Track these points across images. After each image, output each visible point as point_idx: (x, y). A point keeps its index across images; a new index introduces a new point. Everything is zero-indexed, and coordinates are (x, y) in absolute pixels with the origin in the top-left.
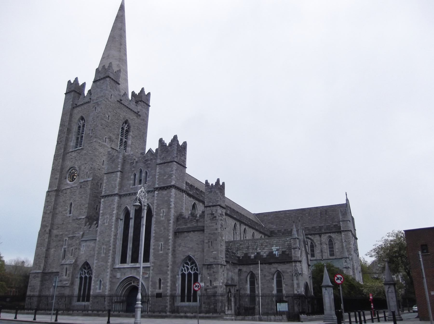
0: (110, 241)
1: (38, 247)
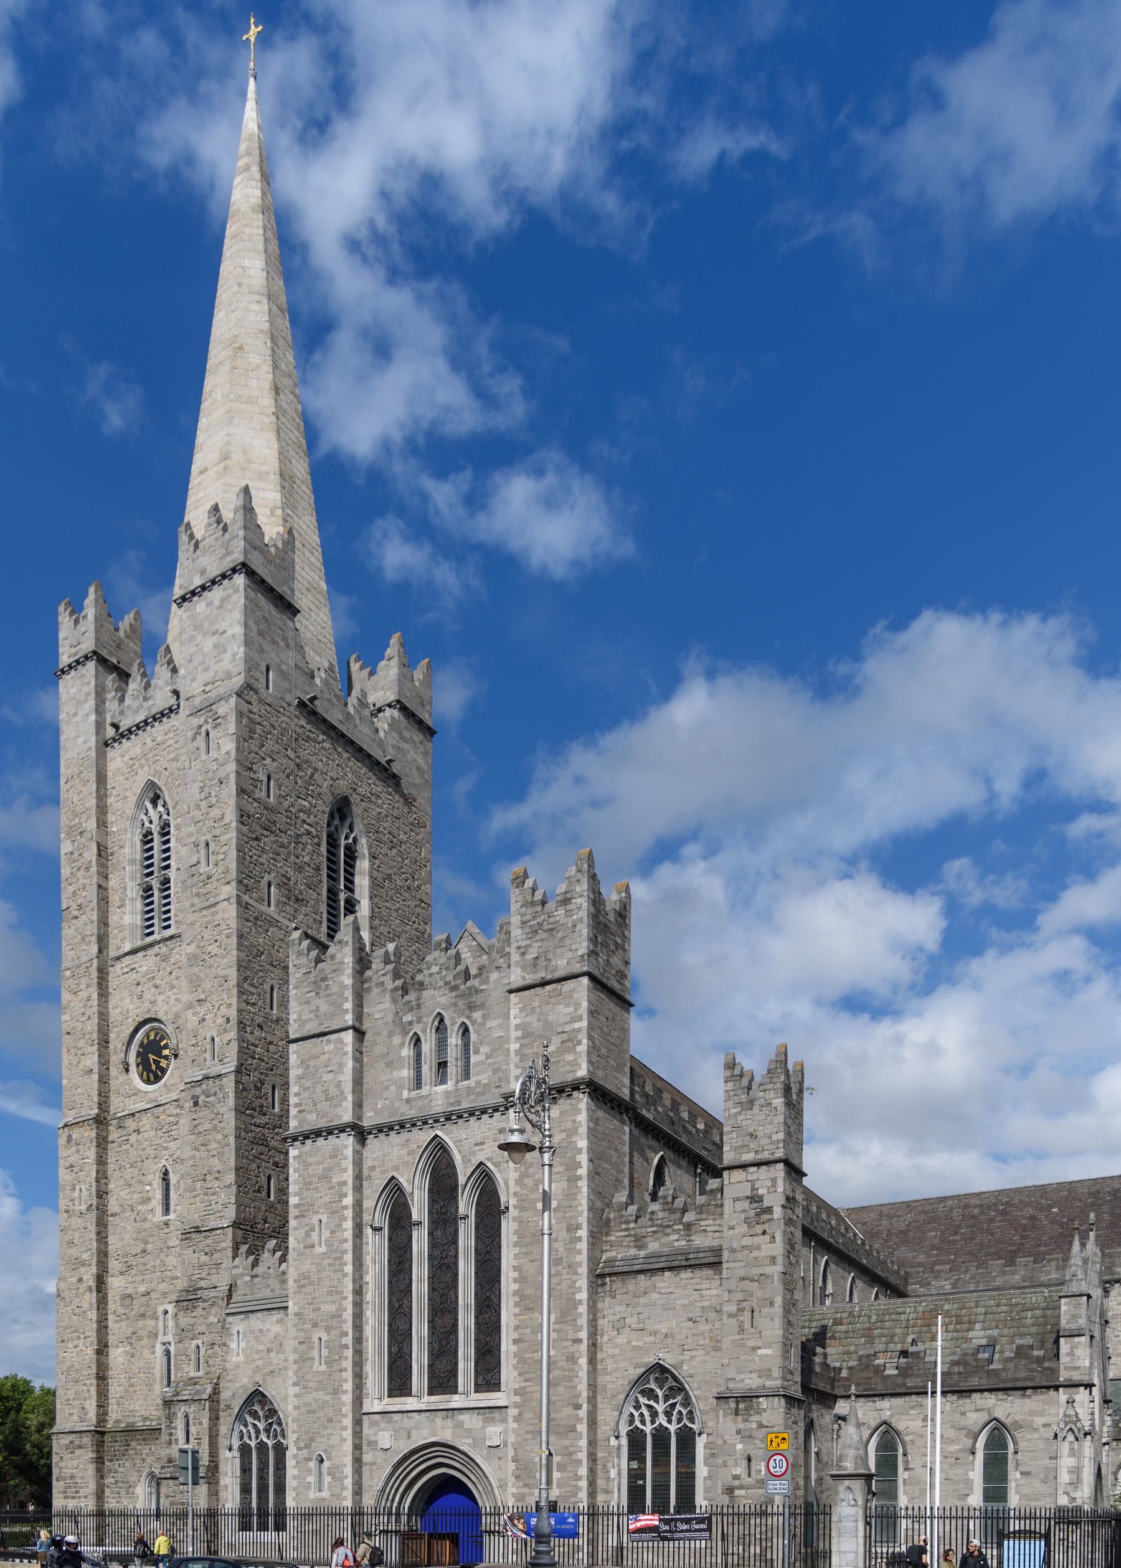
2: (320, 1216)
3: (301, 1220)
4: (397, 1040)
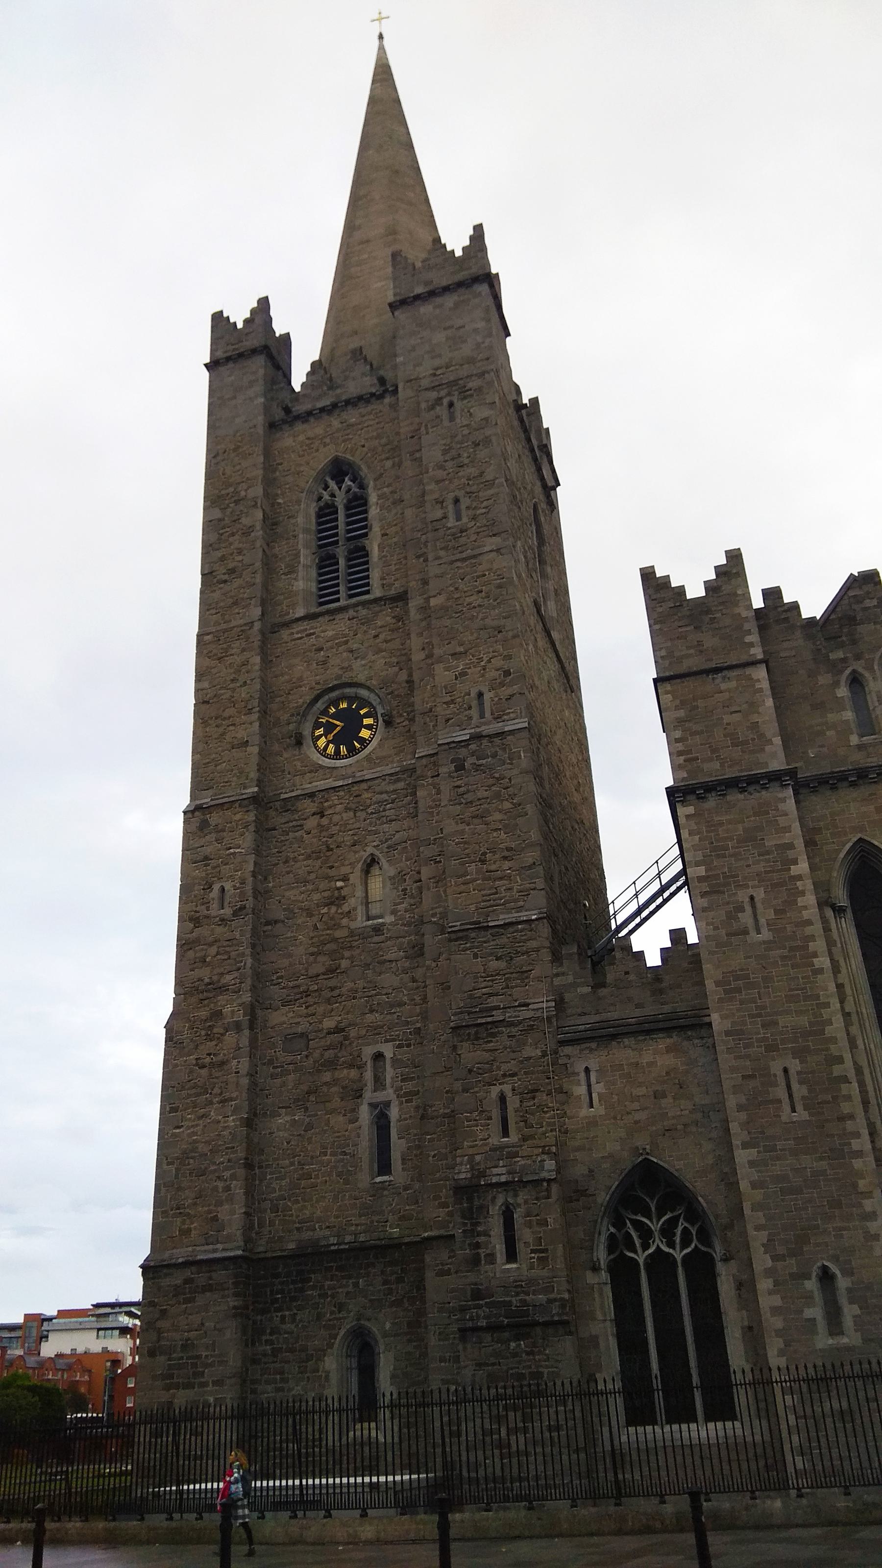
0: (822, 1032)
1: (174, 1110)
2: (751, 891)
3: (715, 897)
4: (824, 679)
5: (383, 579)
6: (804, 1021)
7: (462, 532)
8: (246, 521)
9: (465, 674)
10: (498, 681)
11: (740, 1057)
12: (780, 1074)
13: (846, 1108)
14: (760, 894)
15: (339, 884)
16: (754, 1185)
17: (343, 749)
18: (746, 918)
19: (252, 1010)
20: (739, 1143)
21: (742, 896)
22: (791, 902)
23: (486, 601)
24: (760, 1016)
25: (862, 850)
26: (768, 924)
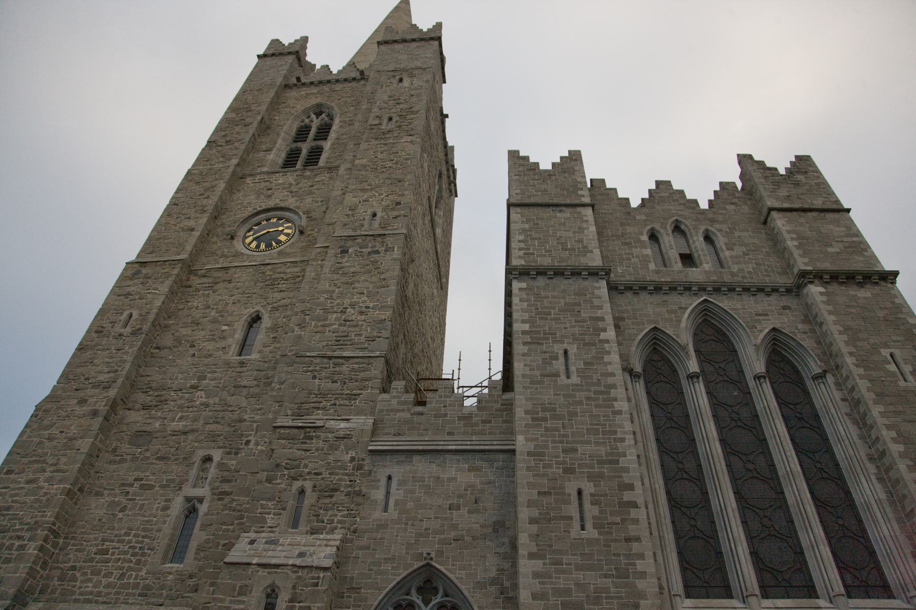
0: (617, 462)
2: (565, 346)
5: (329, 158)
6: (602, 451)
7: (389, 132)
8: (248, 120)
9: (368, 201)
10: (391, 207)
11: (537, 475)
12: (574, 494)
13: (632, 530)
14: (573, 350)
15: (224, 328)
16: (535, 597)
17: (263, 246)
18: (559, 365)
19: (113, 406)
20: (525, 553)
21: (558, 349)
22: (599, 358)
23: (395, 166)
24: (561, 442)
25: (655, 338)
26: (577, 371)
